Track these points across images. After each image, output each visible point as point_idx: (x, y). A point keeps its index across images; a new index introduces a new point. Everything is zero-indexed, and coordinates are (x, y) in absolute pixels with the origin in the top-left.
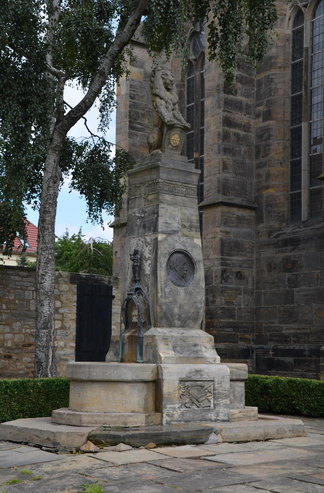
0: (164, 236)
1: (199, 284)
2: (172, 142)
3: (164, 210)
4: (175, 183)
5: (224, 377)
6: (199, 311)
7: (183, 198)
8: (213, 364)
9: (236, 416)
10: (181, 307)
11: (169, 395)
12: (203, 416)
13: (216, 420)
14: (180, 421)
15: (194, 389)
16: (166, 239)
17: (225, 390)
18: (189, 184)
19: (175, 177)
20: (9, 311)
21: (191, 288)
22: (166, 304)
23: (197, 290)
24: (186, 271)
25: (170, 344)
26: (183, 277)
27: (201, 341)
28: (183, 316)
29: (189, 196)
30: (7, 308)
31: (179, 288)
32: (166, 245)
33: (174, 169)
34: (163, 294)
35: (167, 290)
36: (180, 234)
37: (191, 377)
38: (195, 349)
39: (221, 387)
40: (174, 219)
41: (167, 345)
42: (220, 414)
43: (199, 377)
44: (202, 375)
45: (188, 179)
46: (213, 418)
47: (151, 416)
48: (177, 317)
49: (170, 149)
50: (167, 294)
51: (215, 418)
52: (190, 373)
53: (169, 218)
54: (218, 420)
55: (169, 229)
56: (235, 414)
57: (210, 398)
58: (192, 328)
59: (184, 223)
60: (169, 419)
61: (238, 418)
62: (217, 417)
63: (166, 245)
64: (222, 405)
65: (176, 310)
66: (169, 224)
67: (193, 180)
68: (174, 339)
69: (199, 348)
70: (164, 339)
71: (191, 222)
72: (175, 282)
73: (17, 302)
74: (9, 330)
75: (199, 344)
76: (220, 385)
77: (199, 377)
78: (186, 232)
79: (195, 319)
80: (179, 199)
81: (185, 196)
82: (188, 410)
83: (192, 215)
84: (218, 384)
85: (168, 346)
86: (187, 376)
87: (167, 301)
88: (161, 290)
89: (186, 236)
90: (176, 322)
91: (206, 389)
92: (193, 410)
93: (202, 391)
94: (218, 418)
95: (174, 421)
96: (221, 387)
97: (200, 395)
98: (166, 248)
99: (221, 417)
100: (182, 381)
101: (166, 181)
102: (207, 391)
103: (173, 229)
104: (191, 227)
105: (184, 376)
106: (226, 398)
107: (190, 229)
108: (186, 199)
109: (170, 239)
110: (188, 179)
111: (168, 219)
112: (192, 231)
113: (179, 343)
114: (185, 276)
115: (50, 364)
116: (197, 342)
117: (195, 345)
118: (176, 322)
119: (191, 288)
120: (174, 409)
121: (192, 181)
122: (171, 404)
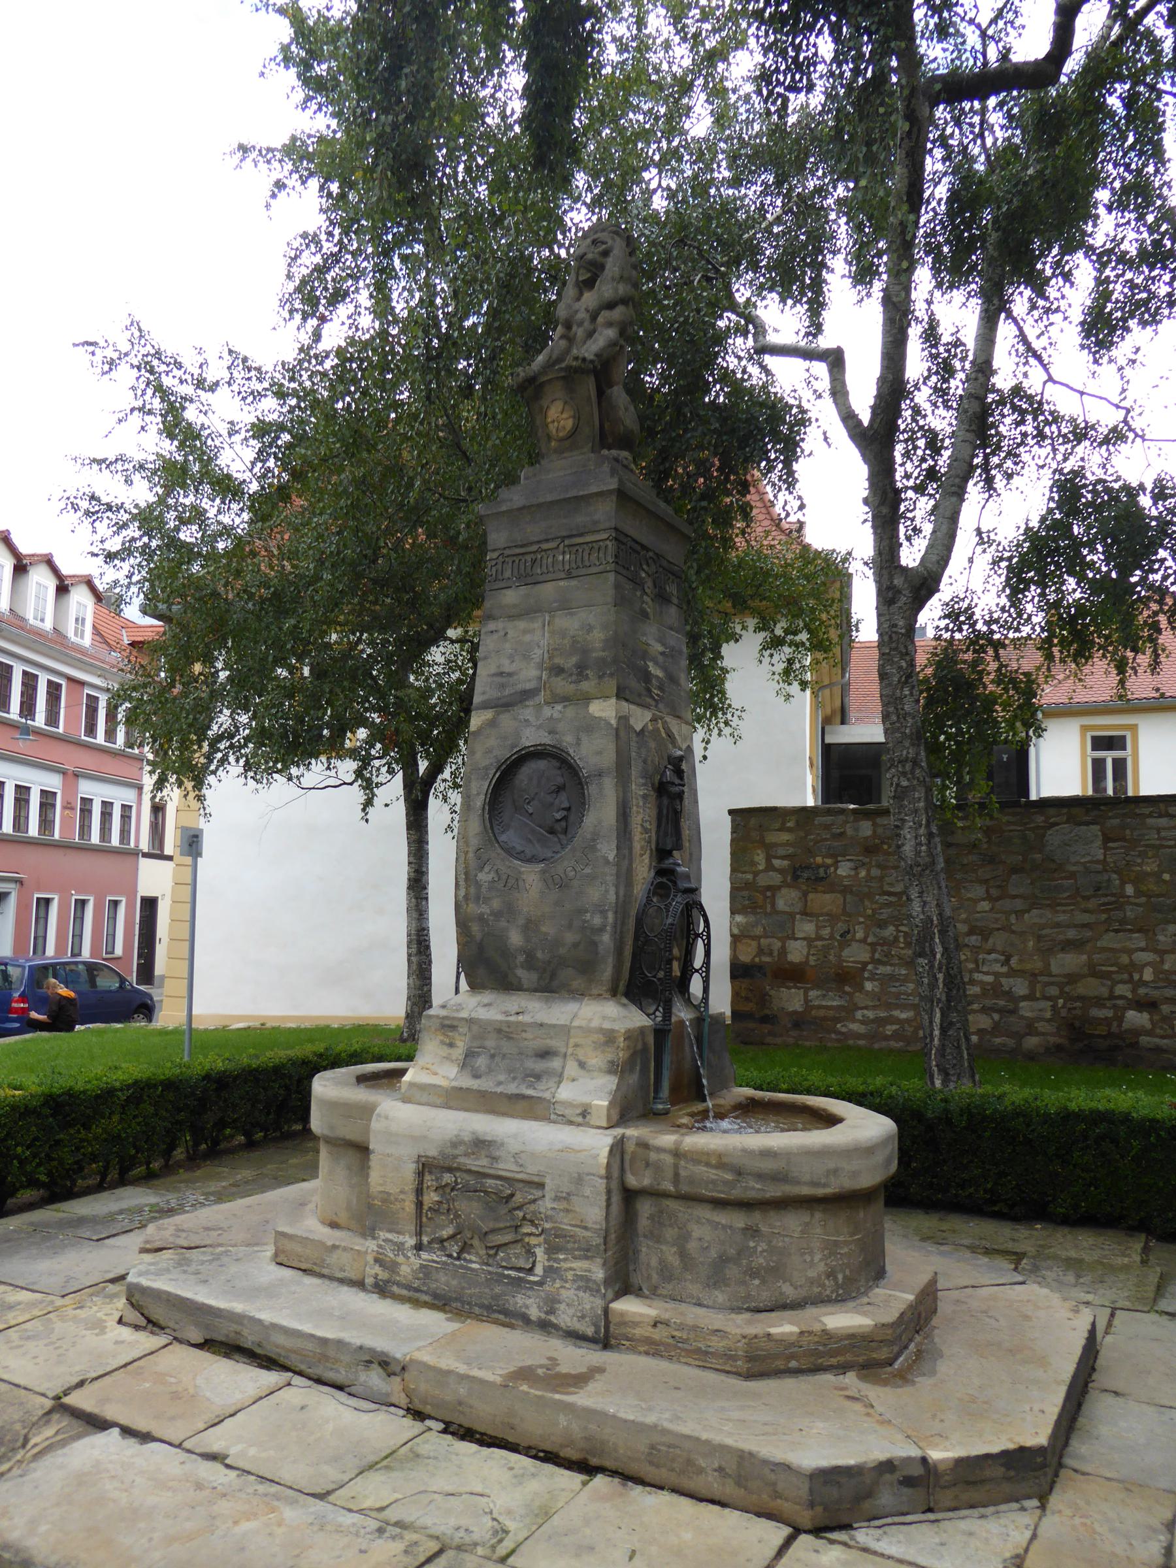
0: (488, 715)
1: (593, 849)
2: (552, 428)
3: (495, 636)
4: (534, 548)
5: (579, 1180)
6: (596, 938)
7: (562, 583)
8: (579, 1125)
9: (638, 1332)
10: (530, 926)
11: (384, 1201)
12: (496, 1297)
13: (545, 1326)
14: (417, 1290)
15: (470, 1199)
16: (492, 723)
17: (586, 1228)
18: (581, 535)
19: (533, 530)
20: (1143, 900)
21: (565, 865)
22: (481, 918)
23: (588, 870)
24: (568, 809)
25: (460, 1044)
26: (552, 831)
27: (572, 1041)
28: (539, 955)
29: (583, 571)
30: (1139, 893)
31: (525, 868)
32: (492, 742)
33: (524, 508)
34: (472, 890)
35: (484, 877)
36: (541, 698)
37: (455, 1157)
38: (540, 1066)
39: (567, 1211)
40: (526, 657)
41: (451, 1045)
42: (562, 1306)
43: (484, 1162)
44: (495, 1159)
45: (580, 519)
46: (534, 1313)
47: (339, 1252)
48: (521, 958)
49: (555, 451)
50: (483, 890)
51: (543, 1316)
52: (454, 1145)
53: (512, 658)
54: (556, 1327)
55: (507, 692)
56: (636, 1324)
57: (533, 1241)
58: (578, 995)
59: (557, 661)
60: (383, 1275)
61: (649, 1341)
62: (547, 1313)
63: (492, 742)
64: (569, 1275)
65: (515, 938)
66: (510, 675)
67: (596, 517)
68: (475, 1028)
69: (556, 1063)
70: (443, 1026)
71: (585, 652)
72: (519, 848)
73: (1166, 877)
74: (1143, 944)
75: (563, 1050)
76: (563, 1205)
77: (484, 1162)
78: (562, 685)
79: (587, 967)
80: (548, 591)
81: (569, 576)
82: (445, 1263)
83: (590, 629)
84: (557, 1199)
85: (451, 1051)
86: (442, 1153)
87: (485, 909)
88: (466, 880)
89: (565, 699)
90: (520, 972)
91: (519, 1208)
92: (462, 1267)
93: (503, 1210)
94: (552, 1318)
95: (398, 1284)
96: (567, 1211)
97: (491, 1225)
98: (489, 751)
99: (565, 1318)
100: (425, 1167)
101: (507, 552)
102: (521, 1214)
103: (520, 687)
104: (581, 670)
105: (433, 1152)
106: (587, 1258)
107: (580, 674)
108: (574, 583)
109: (507, 721)
110: (580, 519)
111: (506, 662)
112: (587, 678)
113: (490, 1043)
114: (558, 827)
115: (936, 1042)
116: (555, 1043)
117: (545, 1054)
118: (520, 972)
119: (566, 863)
120: (400, 1247)
121: (595, 523)
122: (390, 1231)
